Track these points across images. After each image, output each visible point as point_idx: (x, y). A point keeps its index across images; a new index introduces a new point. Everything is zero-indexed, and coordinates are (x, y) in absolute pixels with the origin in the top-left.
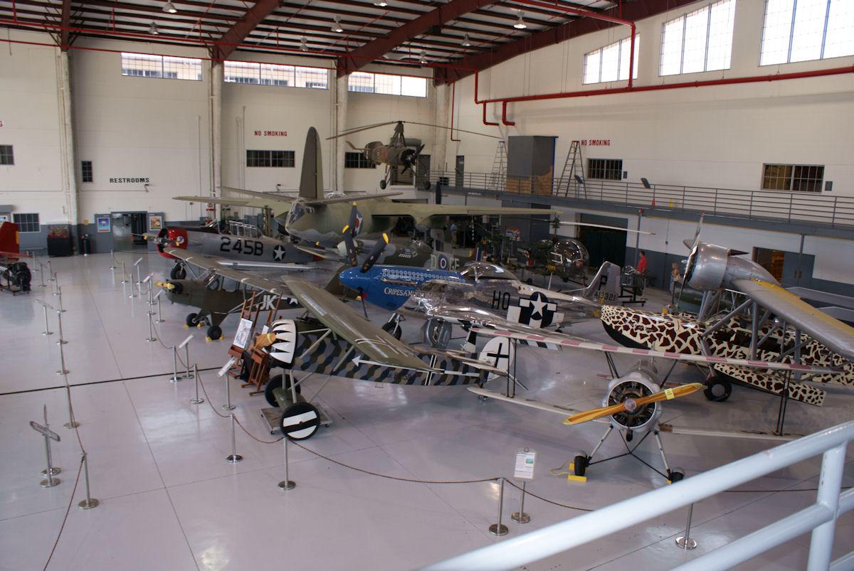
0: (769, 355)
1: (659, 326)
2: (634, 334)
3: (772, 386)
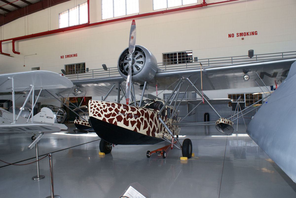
2: (126, 123)
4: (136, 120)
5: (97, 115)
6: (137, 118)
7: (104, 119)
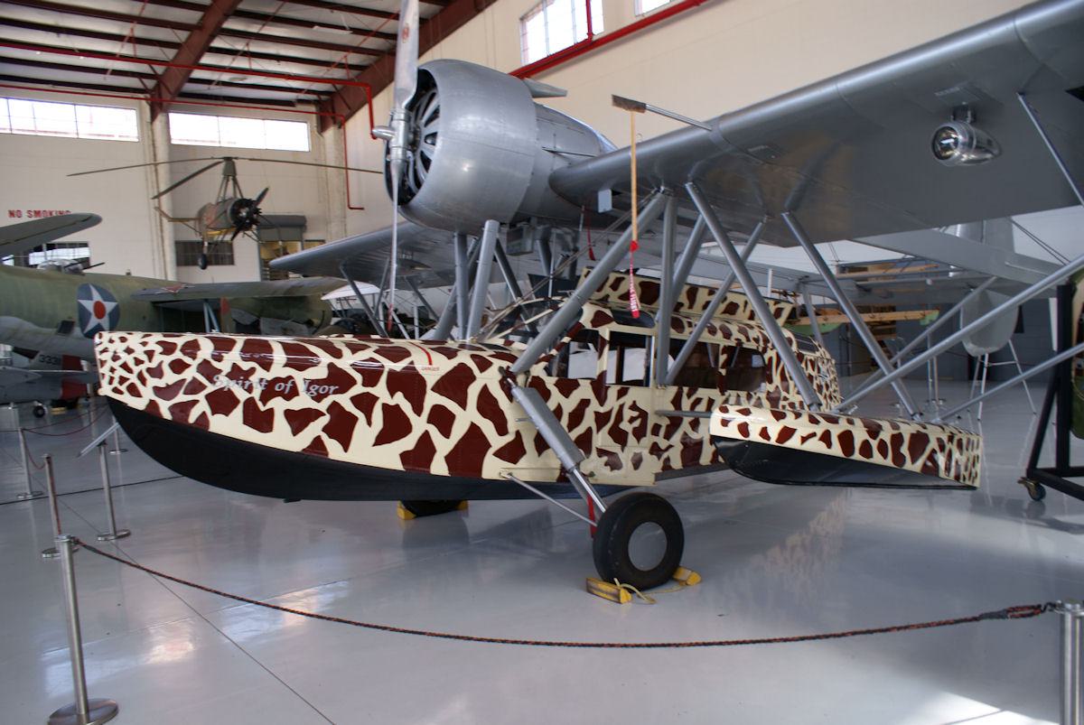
0: (698, 401)
2: (258, 419)
3: (904, 450)
5: (123, 388)
6: (326, 395)
7: (152, 404)
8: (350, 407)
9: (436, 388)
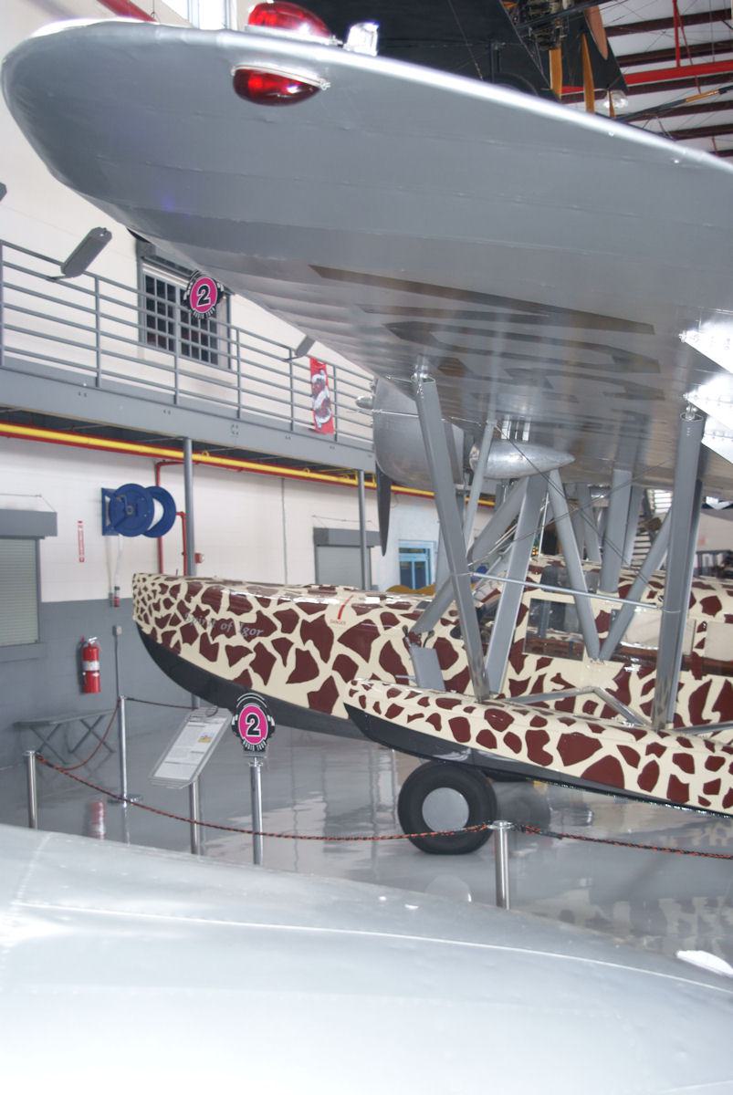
1: (277, 615)
2: (210, 652)
3: (551, 747)
4: (251, 645)
6: (254, 637)
8: (270, 649)
9: (343, 640)
